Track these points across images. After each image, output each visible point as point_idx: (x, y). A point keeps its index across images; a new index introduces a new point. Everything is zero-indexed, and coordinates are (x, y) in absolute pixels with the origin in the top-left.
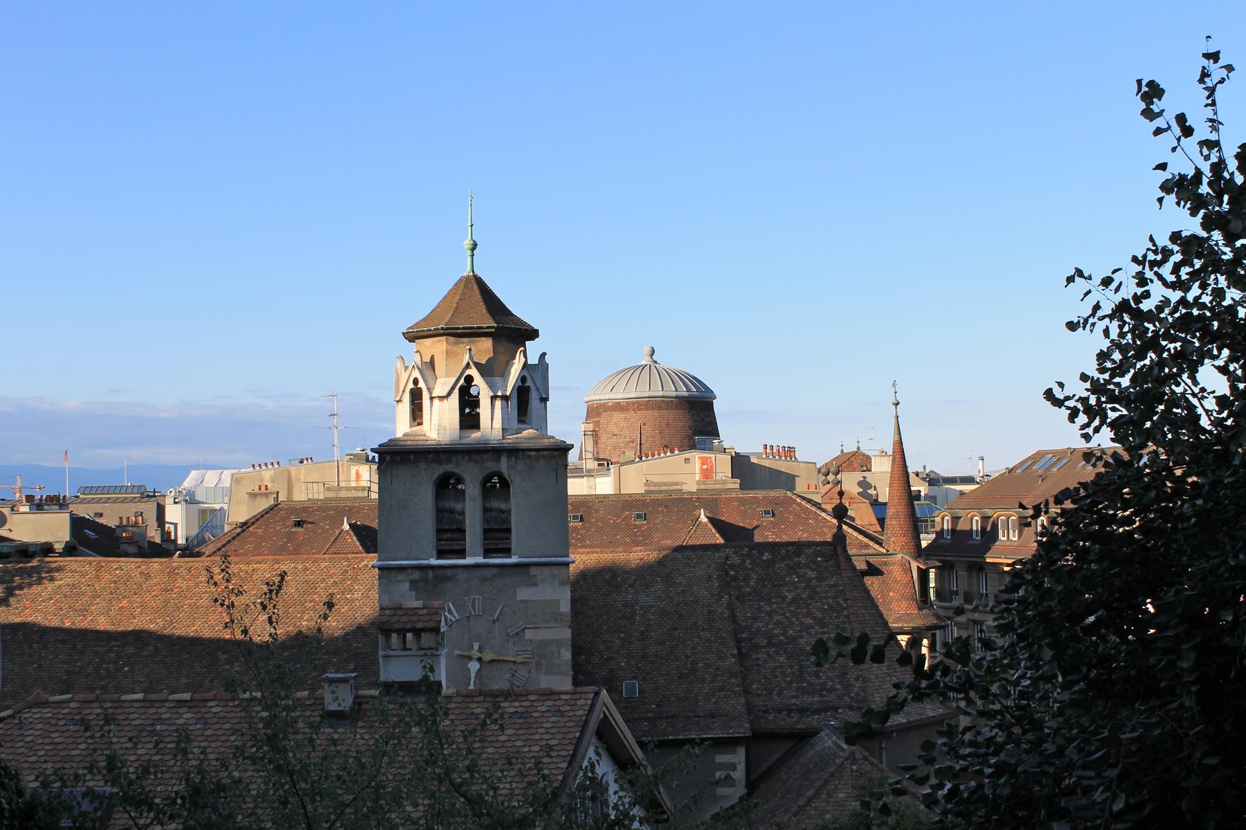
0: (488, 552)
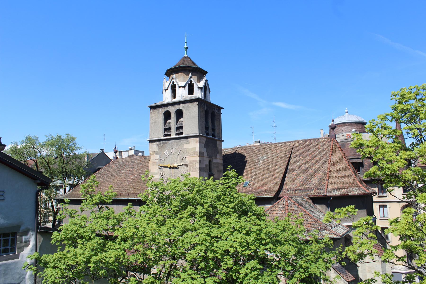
0: (177, 134)
